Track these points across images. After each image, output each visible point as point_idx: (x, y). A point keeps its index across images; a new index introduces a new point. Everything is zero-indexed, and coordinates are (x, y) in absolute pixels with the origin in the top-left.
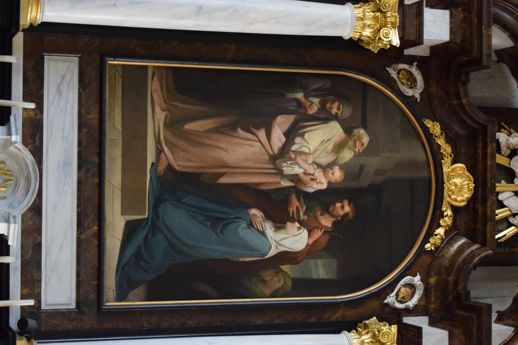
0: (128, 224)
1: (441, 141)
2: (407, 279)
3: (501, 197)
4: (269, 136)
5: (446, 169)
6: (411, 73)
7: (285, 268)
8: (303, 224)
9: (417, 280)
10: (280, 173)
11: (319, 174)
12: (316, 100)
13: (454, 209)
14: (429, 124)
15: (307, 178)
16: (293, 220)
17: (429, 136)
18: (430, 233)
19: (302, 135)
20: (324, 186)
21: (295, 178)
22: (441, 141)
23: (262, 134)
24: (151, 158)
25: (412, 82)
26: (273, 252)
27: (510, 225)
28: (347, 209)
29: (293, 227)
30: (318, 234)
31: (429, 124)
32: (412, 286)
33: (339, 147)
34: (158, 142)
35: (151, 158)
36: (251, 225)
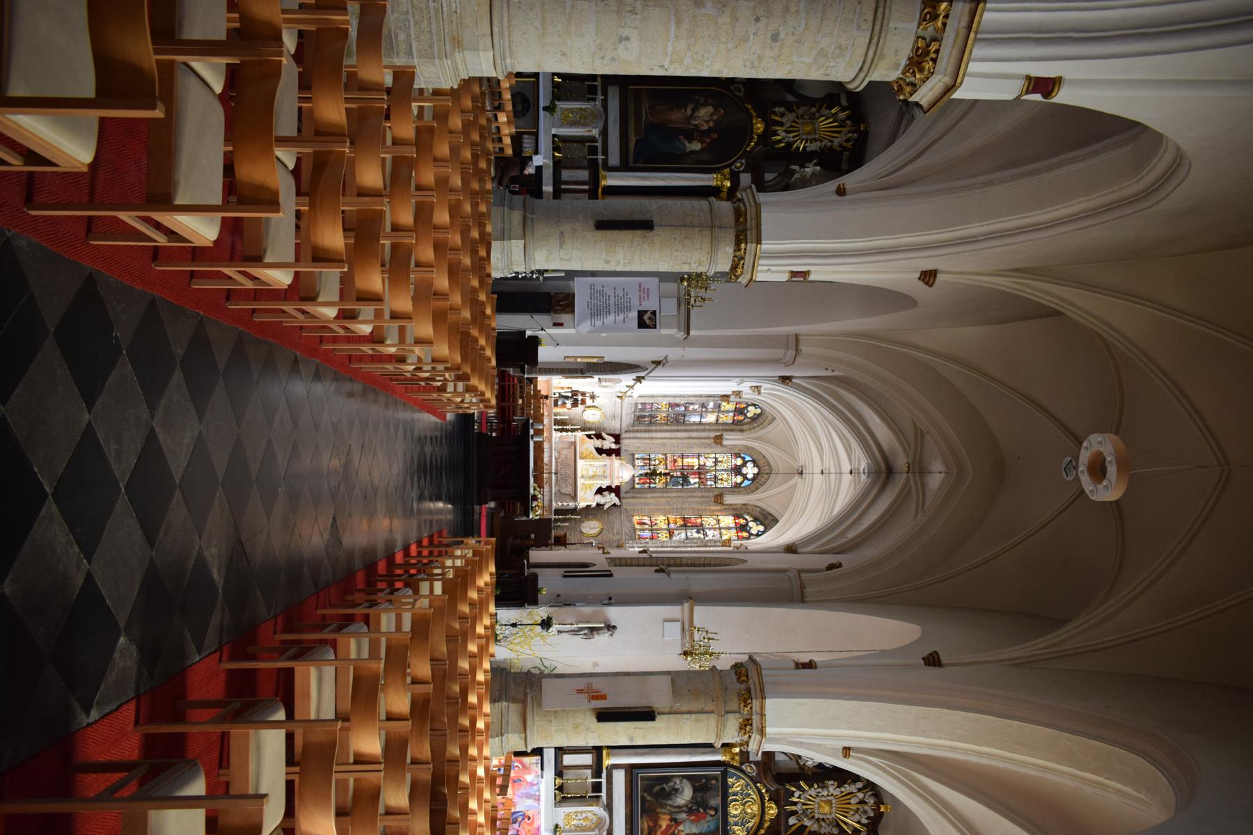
0: (637, 140)
1: (752, 111)
2: (739, 160)
3: (778, 132)
4: (685, 110)
5: (754, 121)
6: (739, 88)
7: (693, 156)
8: (699, 141)
9: (743, 161)
10: (690, 124)
11: (705, 124)
12: (703, 99)
13: (758, 135)
14: (747, 105)
15: (700, 126)
16: (695, 140)
17: (747, 110)
18: (749, 145)
19: (698, 111)
20: (707, 128)
21: (695, 125)
22: (752, 111)
23: (683, 110)
24: (644, 119)
25: (740, 91)
26: (688, 150)
27: (782, 143)
28: (716, 136)
29: (695, 142)
30: (704, 145)
31: (747, 105)
32: (742, 163)
33: (712, 115)
34: (646, 112)
35: (644, 119)
36: (680, 141)
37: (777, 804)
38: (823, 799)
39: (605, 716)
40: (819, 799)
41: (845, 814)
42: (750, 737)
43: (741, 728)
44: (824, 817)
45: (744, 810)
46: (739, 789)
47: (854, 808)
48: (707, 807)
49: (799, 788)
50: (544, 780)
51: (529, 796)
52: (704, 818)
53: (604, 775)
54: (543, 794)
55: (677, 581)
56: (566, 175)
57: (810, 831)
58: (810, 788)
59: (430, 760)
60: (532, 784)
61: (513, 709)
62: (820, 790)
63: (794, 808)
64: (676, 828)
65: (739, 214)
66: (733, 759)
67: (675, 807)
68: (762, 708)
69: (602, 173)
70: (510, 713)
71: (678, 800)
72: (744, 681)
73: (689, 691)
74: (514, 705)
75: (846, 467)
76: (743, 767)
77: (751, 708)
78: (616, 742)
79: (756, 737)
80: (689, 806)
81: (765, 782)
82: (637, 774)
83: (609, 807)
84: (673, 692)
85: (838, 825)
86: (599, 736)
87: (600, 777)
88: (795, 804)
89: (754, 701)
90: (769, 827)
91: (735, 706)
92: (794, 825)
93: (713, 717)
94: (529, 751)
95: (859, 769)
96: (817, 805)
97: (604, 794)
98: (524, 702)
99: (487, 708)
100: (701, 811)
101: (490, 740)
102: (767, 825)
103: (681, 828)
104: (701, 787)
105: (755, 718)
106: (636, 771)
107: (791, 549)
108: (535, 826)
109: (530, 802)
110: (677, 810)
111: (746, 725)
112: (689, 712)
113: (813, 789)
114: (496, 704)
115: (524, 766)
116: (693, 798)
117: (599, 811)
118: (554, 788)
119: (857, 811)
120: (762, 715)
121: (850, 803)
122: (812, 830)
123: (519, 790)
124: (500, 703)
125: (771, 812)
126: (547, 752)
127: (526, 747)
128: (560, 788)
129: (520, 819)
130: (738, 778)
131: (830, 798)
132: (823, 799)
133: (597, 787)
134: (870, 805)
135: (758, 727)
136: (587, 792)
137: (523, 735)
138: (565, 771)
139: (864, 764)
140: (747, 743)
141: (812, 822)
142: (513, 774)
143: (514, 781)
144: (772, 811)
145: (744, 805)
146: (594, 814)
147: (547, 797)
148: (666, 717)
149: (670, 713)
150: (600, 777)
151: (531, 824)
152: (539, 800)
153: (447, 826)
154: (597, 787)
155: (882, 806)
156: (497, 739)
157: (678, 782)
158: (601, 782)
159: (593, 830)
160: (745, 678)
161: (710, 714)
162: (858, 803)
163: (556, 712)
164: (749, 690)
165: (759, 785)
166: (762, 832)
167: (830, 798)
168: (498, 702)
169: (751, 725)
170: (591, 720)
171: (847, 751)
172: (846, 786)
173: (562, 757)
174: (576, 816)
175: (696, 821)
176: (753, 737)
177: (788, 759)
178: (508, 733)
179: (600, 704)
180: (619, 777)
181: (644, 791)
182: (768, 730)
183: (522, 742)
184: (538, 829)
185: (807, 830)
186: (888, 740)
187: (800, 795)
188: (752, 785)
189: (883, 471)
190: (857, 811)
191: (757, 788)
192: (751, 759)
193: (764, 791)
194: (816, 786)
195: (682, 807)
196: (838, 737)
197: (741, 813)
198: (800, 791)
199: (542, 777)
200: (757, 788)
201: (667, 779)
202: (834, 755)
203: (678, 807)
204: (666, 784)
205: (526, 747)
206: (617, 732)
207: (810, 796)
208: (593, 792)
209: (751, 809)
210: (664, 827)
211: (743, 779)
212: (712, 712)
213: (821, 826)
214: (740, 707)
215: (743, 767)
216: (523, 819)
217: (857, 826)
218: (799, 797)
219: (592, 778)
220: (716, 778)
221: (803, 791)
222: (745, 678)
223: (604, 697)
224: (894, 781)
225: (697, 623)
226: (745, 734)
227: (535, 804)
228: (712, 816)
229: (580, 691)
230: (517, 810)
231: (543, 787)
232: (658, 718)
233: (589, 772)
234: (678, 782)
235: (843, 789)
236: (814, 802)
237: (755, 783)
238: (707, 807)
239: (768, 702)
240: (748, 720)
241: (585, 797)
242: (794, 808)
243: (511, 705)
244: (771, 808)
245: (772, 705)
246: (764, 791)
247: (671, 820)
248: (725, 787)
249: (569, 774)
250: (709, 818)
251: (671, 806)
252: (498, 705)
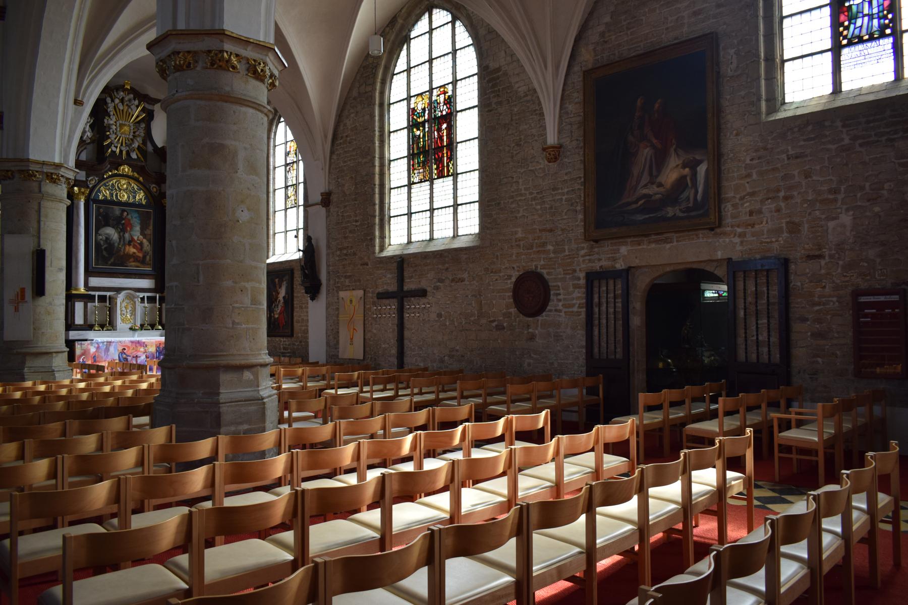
37: (121, 165)
38: (118, 129)
39: (39, 289)
40: (118, 133)
41: (131, 115)
42: (62, 176)
43: (55, 182)
44: (132, 131)
45: (124, 190)
46: (108, 192)
47: (126, 108)
48: (121, 218)
49: (109, 146)
50: (95, 339)
51: (107, 350)
52: (129, 220)
53: (92, 293)
54: (105, 339)
57: (142, 144)
58: (109, 138)
59: (63, 422)
60: (98, 348)
61: (31, 363)
62: (111, 131)
63: (124, 153)
64: (136, 242)
66: (83, 193)
67: (120, 241)
68: (37, 163)
70: (33, 365)
71: (114, 238)
72: (12, 174)
73: (19, 220)
74: (27, 363)
76: (91, 186)
77: (37, 172)
78: (63, 282)
79: (62, 172)
80: (119, 230)
81: (103, 171)
82: (93, 267)
83: (119, 290)
84: (20, 233)
85: (139, 122)
86: (57, 295)
87: (95, 296)
88: (121, 151)
89: (31, 168)
90: (138, 174)
91: (35, 184)
92: (137, 155)
93: (46, 204)
94: (68, 349)
95: (93, 96)
96: (123, 135)
97: (108, 294)
98: (25, 355)
99: (29, 384)
100: (123, 222)
101: (57, 380)
102: (136, 175)
103: (136, 238)
104: (105, 220)
106: (90, 269)
108: (130, 345)
109: (112, 349)
110: (122, 240)
111: (53, 178)
112: (39, 222)
113: (110, 136)
114: (26, 377)
115: (83, 354)
116: (113, 227)
117: (120, 298)
118: (102, 331)
119: (129, 107)
120: (44, 163)
121: (123, 110)
122: (141, 142)
123: (102, 358)
124: (26, 374)
125: (126, 170)
126: (72, 336)
127: (65, 352)
128: (102, 326)
129: (124, 356)
130: (99, 191)
131: (118, 125)
132: (118, 129)
133: (102, 299)
134: (124, 96)
135: (54, 169)
136: (106, 306)
137: (54, 355)
138: (89, 323)
139: (89, 91)
140: (68, 179)
141: (135, 141)
142: (89, 362)
143: (95, 361)
144: (126, 169)
145: (120, 190)
146: (123, 301)
147: (108, 337)
148: (42, 241)
149: (39, 238)
150: (95, 296)
151: (128, 347)
152: (110, 342)
153: (120, 405)
155: (126, 87)
156: (56, 375)
157: (101, 237)
158: (98, 295)
159: (135, 302)
160: (10, 173)
161: (42, 206)
162: (123, 105)
163: (34, 329)
164: (21, 171)
165: (105, 176)
166: (141, 179)
167: (118, 125)
168: (24, 375)
169: (52, 174)
170: (43, 301)
171: (78, 102)
172: (109, 110)
173: (77, 325)
174: (124, 314)
175: (132, 227)
176: (63, 174)
177: (85, 151)
178: (52, 367)
179: (29, 293)
180: (95, 281)
181: (107, 263)
182: (57, 160)
183: (60, 355)
184: (132, 342)
185: (141, 146)
186: (69, 67)
187: (114, 146)
188: (105, 181)
190: (129, 107)
191: (107, 178)
192: (84, 179)
193: (110, 173)
194: (108, 133)
195: (120, 236)
196: (65, 107)
197: (126, 193)
198: (111, 146)
199: (92, 340)
200: (107, 178)
201: (98, 245)
202: (81, 113)
203: (120, 239)
204: (101, 246)
205: (65, 352)
206: (54, 281)
207: (115, 138)
208: (106, 302)
209: (124, 184)
210: (135, 250)
211: (100, 187)
212: (40, 203)
213: (139, 136)
214: (36, 181)
215: (91, 186)
216: (125, 353)
217: (140, 109)
218: (117, 147)
219: (95, 302)
220: (98, 209)
221: (111, 143)
222: (10, 173)
223: (23, 290)
224: (104, 71)
226: (59, 180)
227: (113, 344)
228: (128, 215)
229: (17, 309)
230: (117, 358)
231: (100, 340)
232: (43, 247)
233: (89, 304)
234: (101, 237)
235: (112, 113)
236: (120, 137)
237: (104, 179)
238: (121, 218)
239: (32, 157)
240: (48, 176)
241: (110, 308)
242: (124, 153)
243: (27, 365)
244: (123, 169)
245: (35, 153)
246: (110, 173)
247: (129, 245)
248: (106, 201)
249: (91, 320)
250: (129, 217)
251: (119, 244)
252: (27, 375)
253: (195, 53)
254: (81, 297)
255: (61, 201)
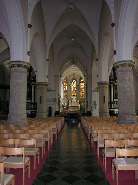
39: (104, 102)
55: (89, 92)
56: (32, 108)
65: (39, 85)
69: (32, 103)
75: (73, 68)
79: (107, 83)
105: (104, 83)
107: (84, 76)
111: (105, 84)
120: (104, 82)
133: (116, 103)
154: (116, 103)
171: (109, 71)
180: (115, 100)
182: (106, 81)
189: (73, 62)
225: (94, 89)
233: (114, 104)
253: (119, 65)
254: (113, 103)
255: (107, 87)
